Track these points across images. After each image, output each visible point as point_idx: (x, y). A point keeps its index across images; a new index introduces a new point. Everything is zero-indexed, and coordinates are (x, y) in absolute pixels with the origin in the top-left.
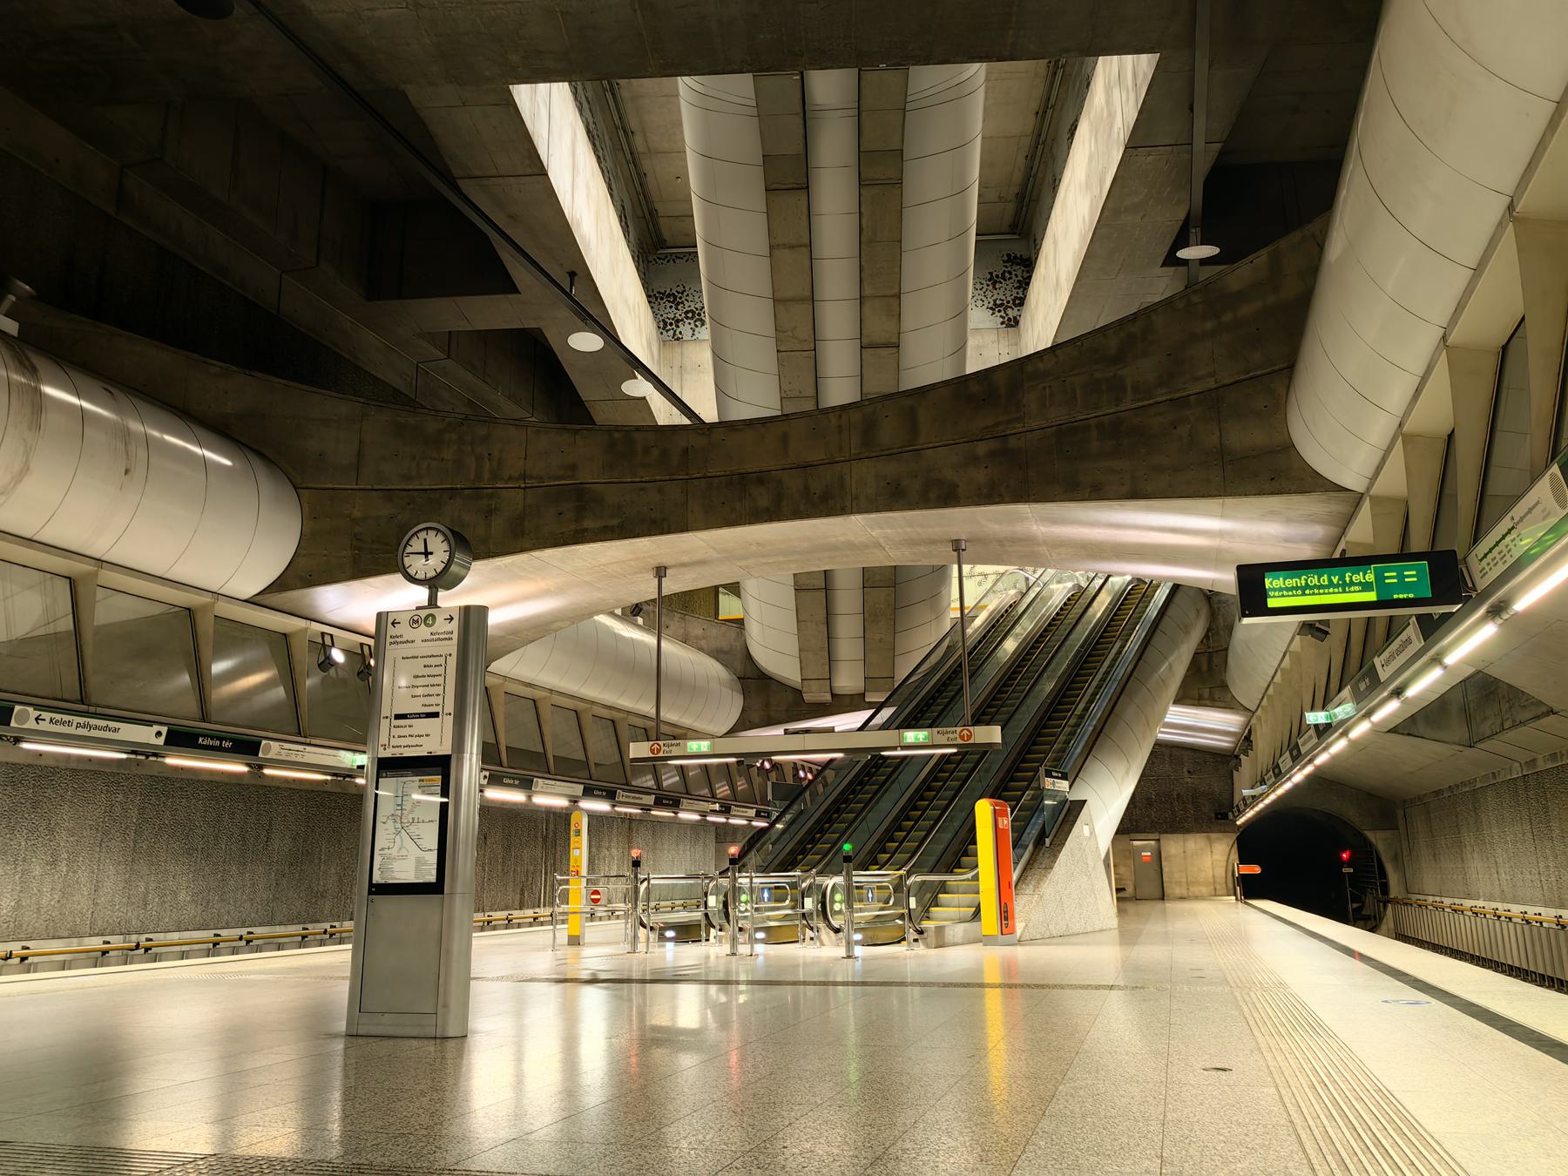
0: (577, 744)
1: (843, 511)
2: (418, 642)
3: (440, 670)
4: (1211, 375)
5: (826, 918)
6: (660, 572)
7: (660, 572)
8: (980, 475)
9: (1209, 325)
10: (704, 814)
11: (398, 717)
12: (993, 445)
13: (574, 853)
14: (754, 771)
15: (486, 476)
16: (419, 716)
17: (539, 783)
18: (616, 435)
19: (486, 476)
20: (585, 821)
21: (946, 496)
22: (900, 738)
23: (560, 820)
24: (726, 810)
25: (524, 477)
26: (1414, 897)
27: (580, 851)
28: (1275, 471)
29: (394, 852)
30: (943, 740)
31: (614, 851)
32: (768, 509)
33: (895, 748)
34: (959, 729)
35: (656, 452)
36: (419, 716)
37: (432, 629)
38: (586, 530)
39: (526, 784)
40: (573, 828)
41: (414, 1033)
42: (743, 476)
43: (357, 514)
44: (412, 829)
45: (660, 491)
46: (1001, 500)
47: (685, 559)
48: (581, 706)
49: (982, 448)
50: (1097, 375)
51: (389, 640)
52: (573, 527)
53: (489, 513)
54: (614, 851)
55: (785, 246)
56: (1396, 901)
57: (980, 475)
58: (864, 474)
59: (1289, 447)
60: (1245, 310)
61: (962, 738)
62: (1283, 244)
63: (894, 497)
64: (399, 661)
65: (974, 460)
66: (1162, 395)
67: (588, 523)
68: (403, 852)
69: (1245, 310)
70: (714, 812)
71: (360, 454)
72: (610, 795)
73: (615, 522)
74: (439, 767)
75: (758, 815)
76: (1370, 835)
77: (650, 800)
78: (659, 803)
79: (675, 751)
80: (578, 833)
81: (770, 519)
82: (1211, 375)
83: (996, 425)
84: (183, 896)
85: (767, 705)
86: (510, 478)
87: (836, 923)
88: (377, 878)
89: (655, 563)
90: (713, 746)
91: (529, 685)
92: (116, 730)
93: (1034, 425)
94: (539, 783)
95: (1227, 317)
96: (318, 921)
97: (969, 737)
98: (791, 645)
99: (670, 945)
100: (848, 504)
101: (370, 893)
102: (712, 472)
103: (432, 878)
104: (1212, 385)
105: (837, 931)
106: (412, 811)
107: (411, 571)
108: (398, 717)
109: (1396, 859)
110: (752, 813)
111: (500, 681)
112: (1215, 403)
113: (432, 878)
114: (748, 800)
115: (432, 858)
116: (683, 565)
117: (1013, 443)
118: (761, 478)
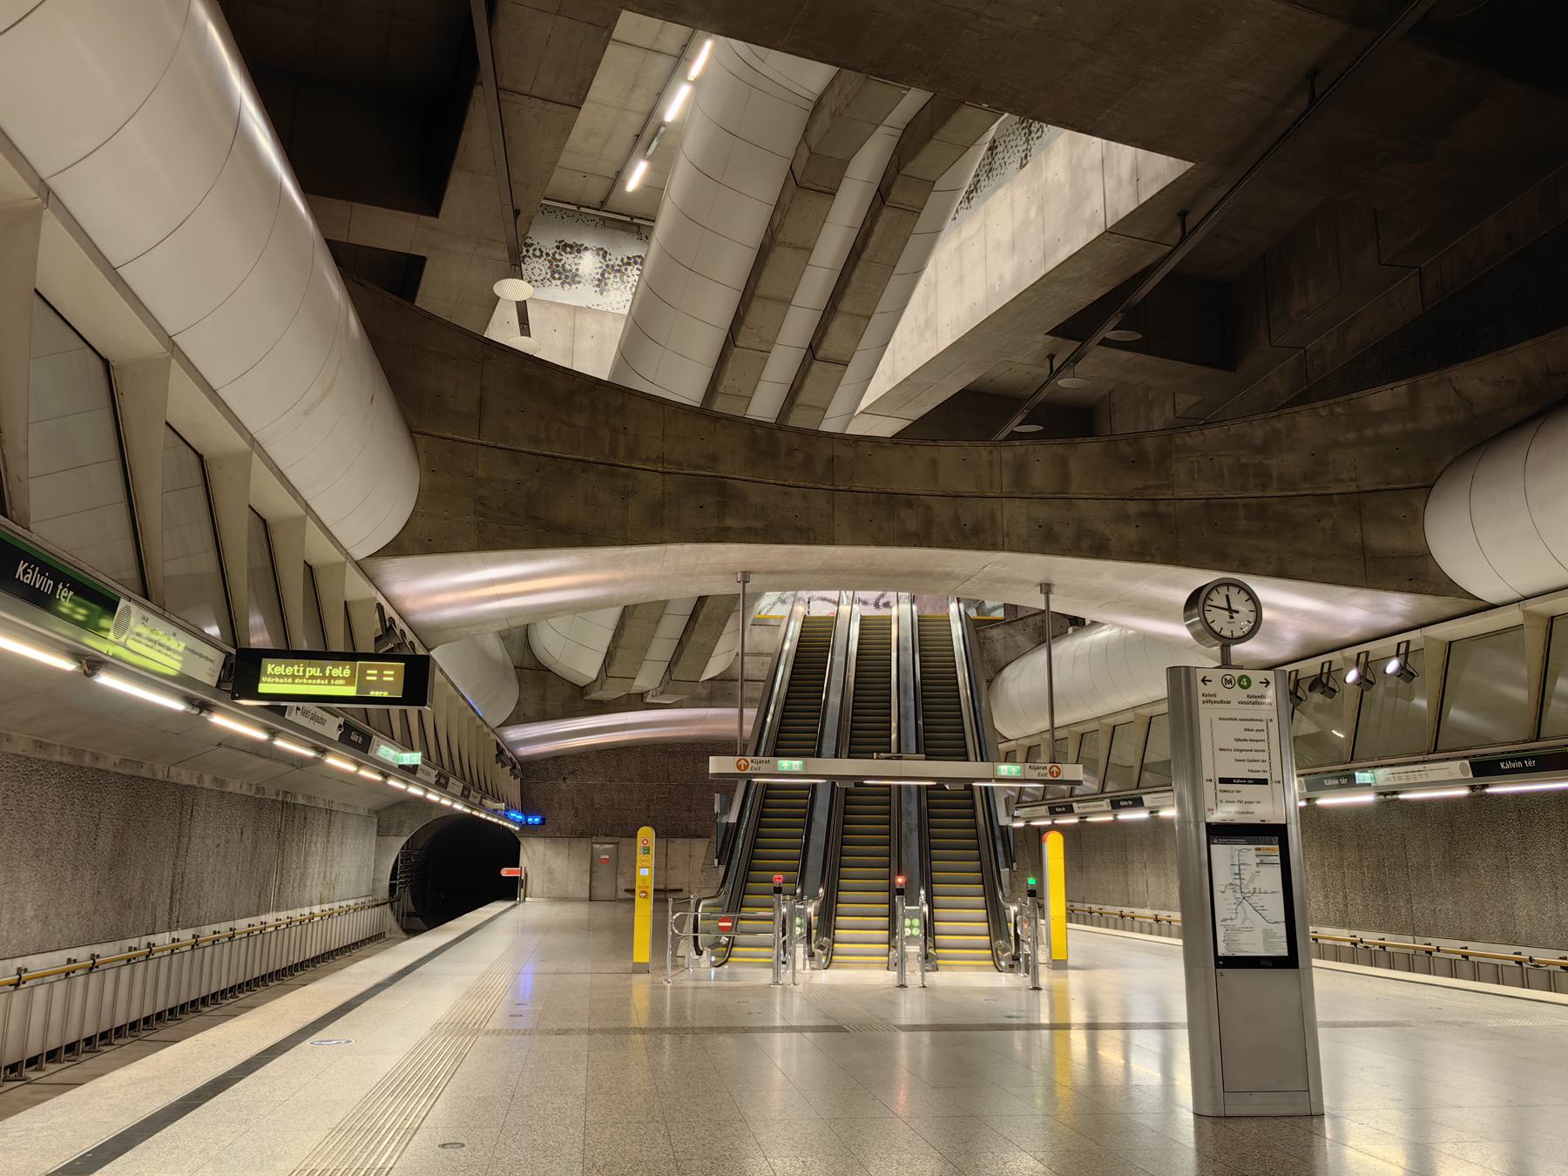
1: (994, 547)
2: (1234, 703)
3: (1263, 736)
4: (1351, 480)
8: (1132, 534)
9: (1351, 436)
11: (1222, 781)
12: (1144, 506)
15: (622, 452)
16: (1246, 781)
18: (759, 431)
19: (622, 452)
21: (1100, 550)
22: (994, 770)
25: (662, 459)
28: (1413, 570)
29: (1238, 923)
30: (1034, 775)
32: (917, 534)
33: (989, 780)
35: (799, 456)
36: (1246, 781)
37: (1249, 691)
38: (729, 529)
41: (1289, 1112)
42: (891, 495)
43: (480, 473)
44: (1255, 899)
45: (805, 497)
46: (1151, 559)
49: (1132, 508)
50: (1243, 460)
51: (1201, 699)
52: (715, 523)
53: (626, 494)
55: (790, 245)
57: (1132, 534)
58: (1014, 514)
59: (1427, 555)
60: (1386, 429)
62: (1422, 380)
63: (1047, 541)
64: (1216, 720)
65: (1124, 518)
66: (1306, 489)
67: (730, 522)
68: (1247, 924)
69: (1386, 429)
71: (481, 402)
73: (758, 524)
74: (1274, 833)
79: (764, 769)
81: (920, 545)
82: (1351, 480)
83: (1146, 488)
84: (29, 912)
85: (543, 698)
86: (648, 459)
88: (1222, 951)
89: (740, 569)
90: (805, 765)
92: (322, 722)
93: (1182, 494)
95: (1369, 433)
96: (122, 938)
100: (999, 540)
101: (1217, 966)
102: (859, 486)
103: (1283, 951)
104: (1354, 489)
106: (1251, 880)
107: (1237, 634)
108: (1222, 781)
112: (1356, 503)
113: (1283, 951)
115: (1281, 930)
117: (1162, 508)
118: (910, 500)
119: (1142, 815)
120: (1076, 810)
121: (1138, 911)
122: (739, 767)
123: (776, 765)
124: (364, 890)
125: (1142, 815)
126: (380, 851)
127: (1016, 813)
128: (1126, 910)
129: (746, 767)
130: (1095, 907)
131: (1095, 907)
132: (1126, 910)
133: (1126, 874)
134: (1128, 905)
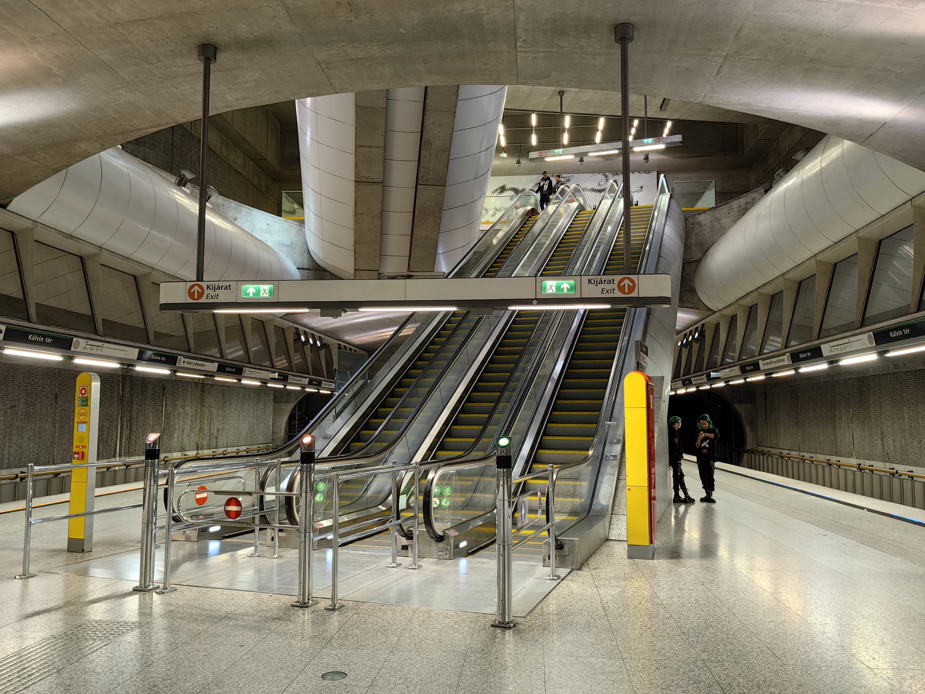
0: (134, 305)
5: (428, 521)
6: (208, 52)
7: (208, 52)
10: (264, 382)
13: (79, 430)
14: (307, 348)
17: (80, 344)
20: (96, 385)
22: (538, 287)
23: (65, 379)
24: (284, 379)
26: (760, 449)
27: (88, 427)
30: (595, 291)
31: (188, 409)
33: (528, 302)
34: (617, 278)
39: (62, 344)
40: (78, 395)
47: (242, 29)
48: (138, 271)
54: (188, 409)
56: (752, 452)
61: (622, 289)
70: (273, 380)
72: (170, 361)
75: (311, 383)
76: (737, 406)
77: (213, 367)
78: (222, 369)
80: (86, 402)
87: (439, 528)
91: (71, 237)
94: (80, 344)
97: (632, 289)
98: (348, 238)
99: (214, 546)
105: (440, 539)
109: (752, 423)
110: (306, 381)
111: (29, 224)
114: (302, 370)
116: (242, 45)
119: (823, 366)
120: (762, 367)
121: (843, 460)
122: (191, 295)
123: (238, 291)
124: (261, 439)
125: (823, 366)
126: (276, 414)
127: (713, 374)
128: (834, 459)
129: (201, 295)
130: (807, 455)
131: (807, 455)
132: (834, 459)
133: (834, 428)
134: (837, 454)
